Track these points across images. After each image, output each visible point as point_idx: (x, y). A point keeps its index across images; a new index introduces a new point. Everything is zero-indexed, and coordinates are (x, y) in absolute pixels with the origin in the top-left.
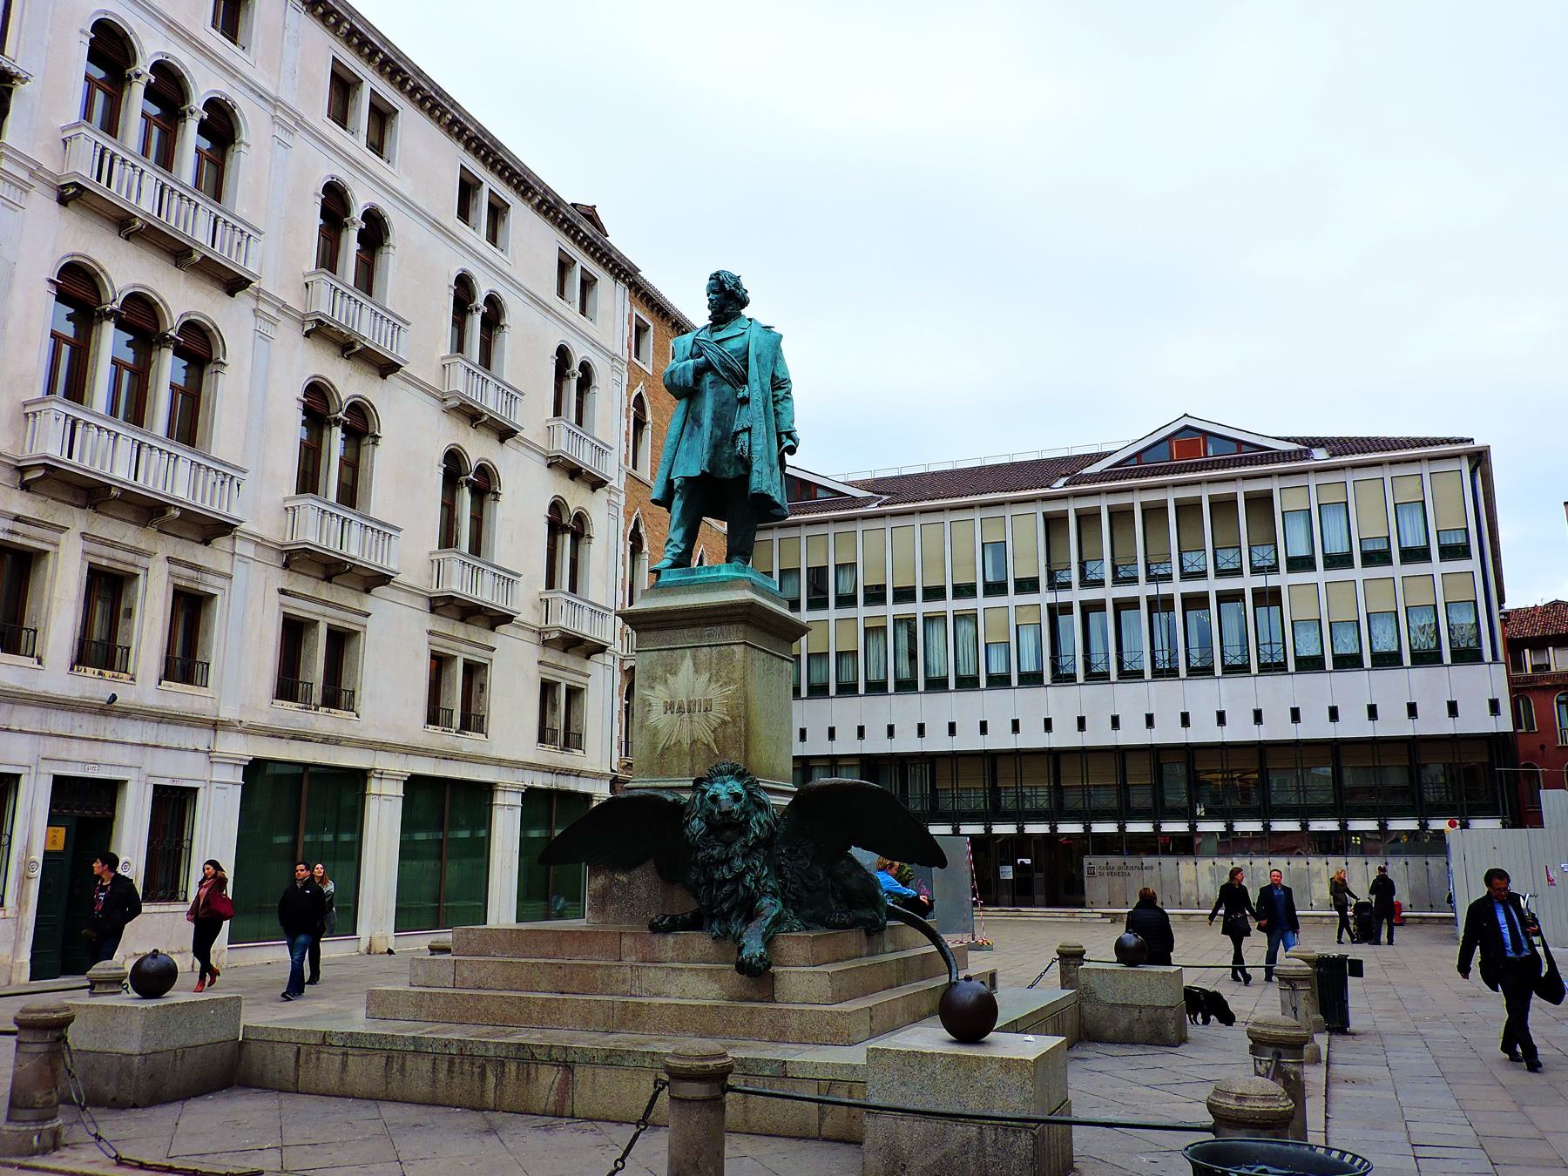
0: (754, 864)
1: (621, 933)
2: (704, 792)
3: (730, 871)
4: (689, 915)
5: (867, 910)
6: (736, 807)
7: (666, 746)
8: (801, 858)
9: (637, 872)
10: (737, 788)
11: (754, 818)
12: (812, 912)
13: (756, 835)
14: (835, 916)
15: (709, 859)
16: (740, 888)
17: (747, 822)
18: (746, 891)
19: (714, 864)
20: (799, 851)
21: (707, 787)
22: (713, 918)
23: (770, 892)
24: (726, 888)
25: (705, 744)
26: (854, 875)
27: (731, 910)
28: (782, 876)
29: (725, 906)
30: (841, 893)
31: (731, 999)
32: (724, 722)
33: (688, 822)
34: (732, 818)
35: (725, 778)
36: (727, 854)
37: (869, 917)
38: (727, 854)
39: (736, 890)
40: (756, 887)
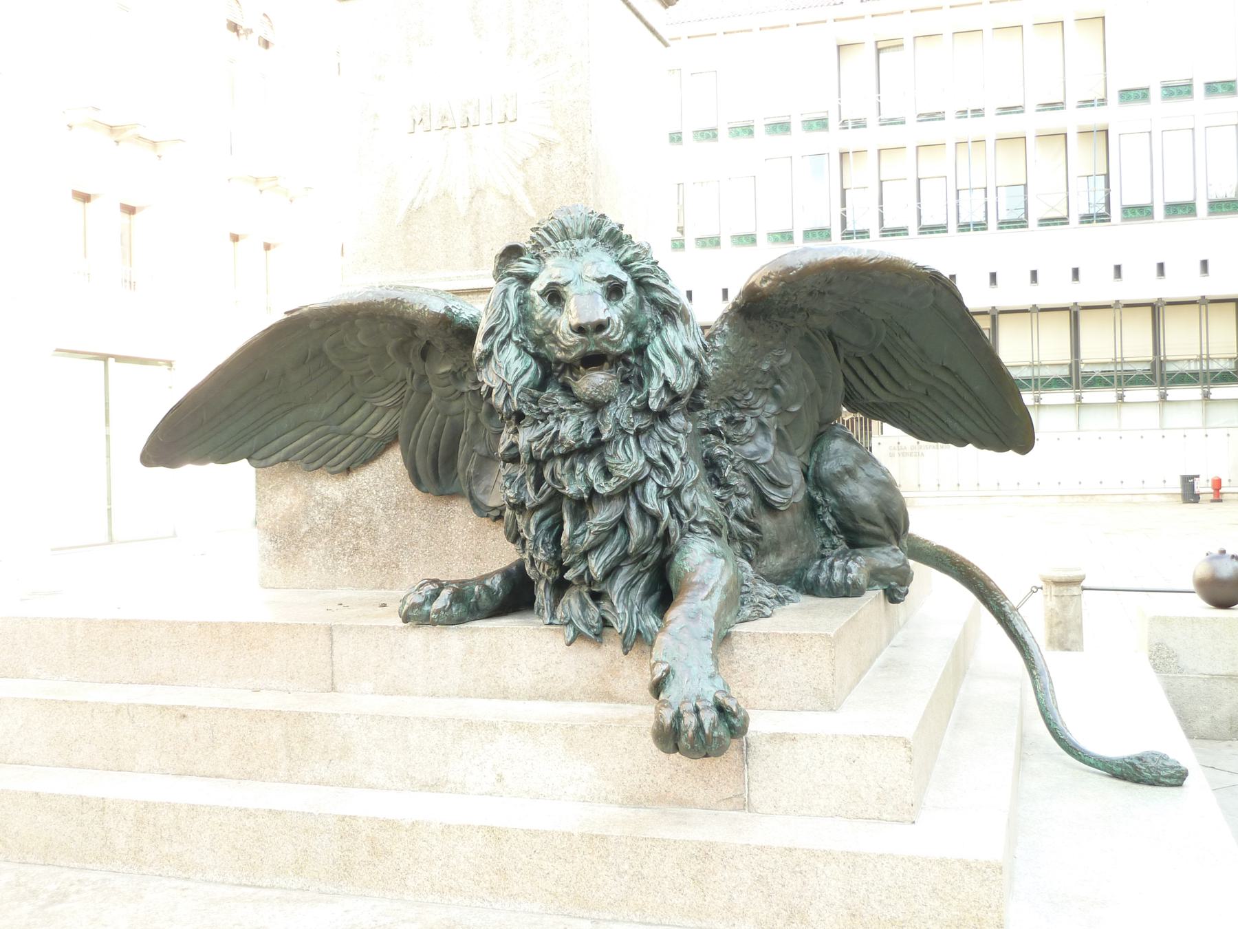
0: (664, 457)
1: (330, 629)
2: (526, 280)
3: (607, 474)
4: (496, 582)
5: (887, 549)
6: (613, 313)
7: (416, 205)
8: (751, 438)
9: (366, 477)
10: (608, 266)
11: (658, 341)
12: (782, 560)
13: (666, 384)
14: (831, 567)
15: (552, 442)
16: (633, 515)
17: (640, 350)
18: (649, 523)
19: (564, 457)
20: (748, 425)
21: (530, 269)
22: (560, 587)
23: (706, 523)
24: (602, 516)
25: (504, 196)
26: (860, 474)
27: (610, 573)
28: (724, 485)
29: (596, 565)
30: (833, 514)
31: (633, 801)
32: (547, 145)
33: (488, 355)
34: (607, 339)
35: (578, 244)
36: (597, 433)
37: (893, 565)
38: (597, 433)
39: (623, 521)
40: (673, 512)
